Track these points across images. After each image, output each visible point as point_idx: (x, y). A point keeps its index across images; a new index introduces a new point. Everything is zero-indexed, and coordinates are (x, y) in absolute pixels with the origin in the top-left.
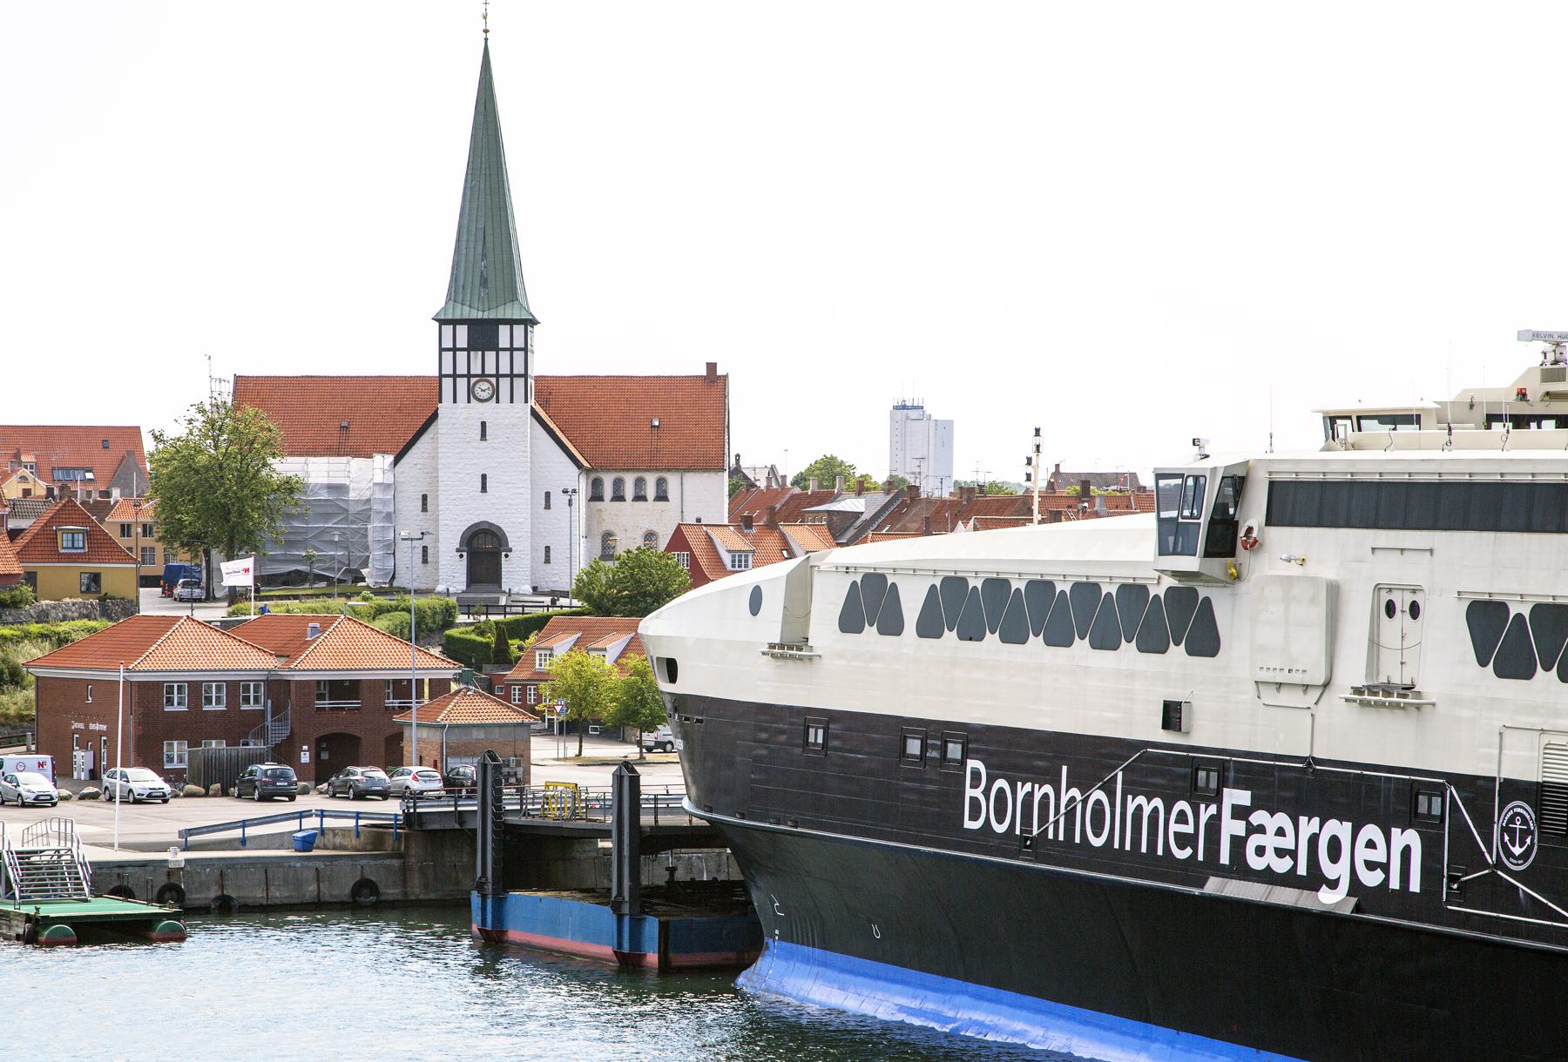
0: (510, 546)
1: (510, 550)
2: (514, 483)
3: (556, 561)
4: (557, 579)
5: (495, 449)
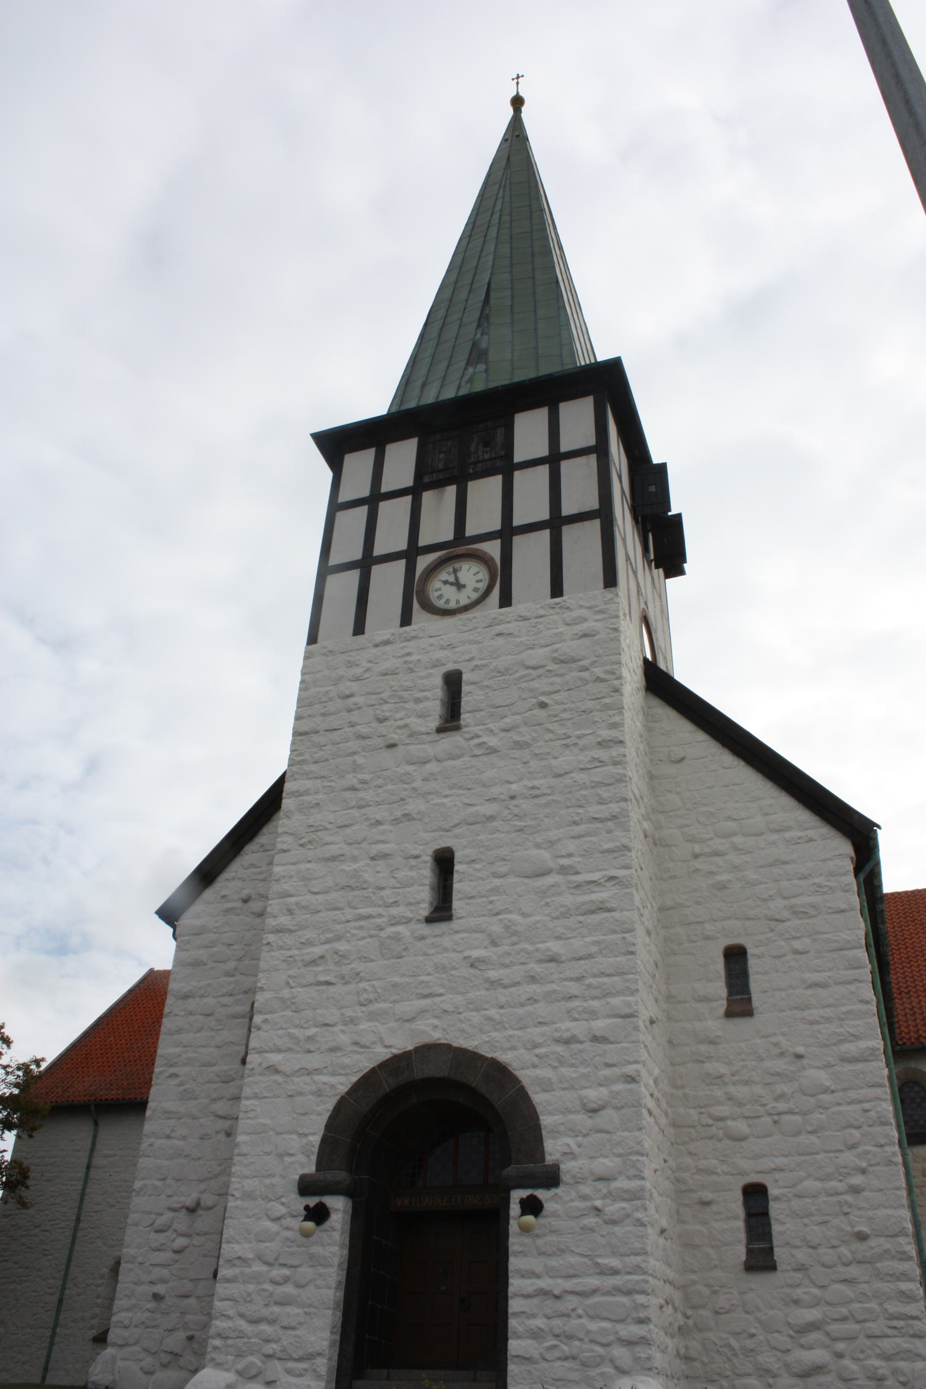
0: (549, 1159)
1: (551, 1178)
2: (564, 870)
3: (801, 1255)
4: (819, 1356)
5: (493, 751)
